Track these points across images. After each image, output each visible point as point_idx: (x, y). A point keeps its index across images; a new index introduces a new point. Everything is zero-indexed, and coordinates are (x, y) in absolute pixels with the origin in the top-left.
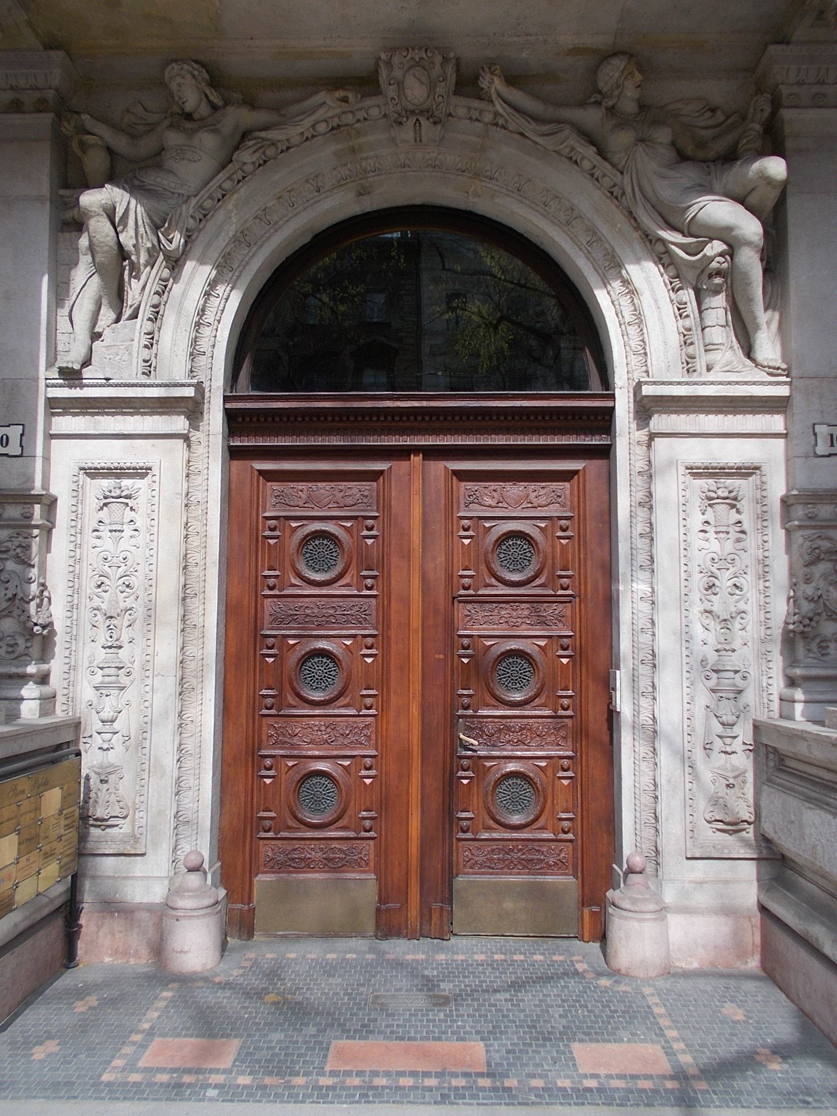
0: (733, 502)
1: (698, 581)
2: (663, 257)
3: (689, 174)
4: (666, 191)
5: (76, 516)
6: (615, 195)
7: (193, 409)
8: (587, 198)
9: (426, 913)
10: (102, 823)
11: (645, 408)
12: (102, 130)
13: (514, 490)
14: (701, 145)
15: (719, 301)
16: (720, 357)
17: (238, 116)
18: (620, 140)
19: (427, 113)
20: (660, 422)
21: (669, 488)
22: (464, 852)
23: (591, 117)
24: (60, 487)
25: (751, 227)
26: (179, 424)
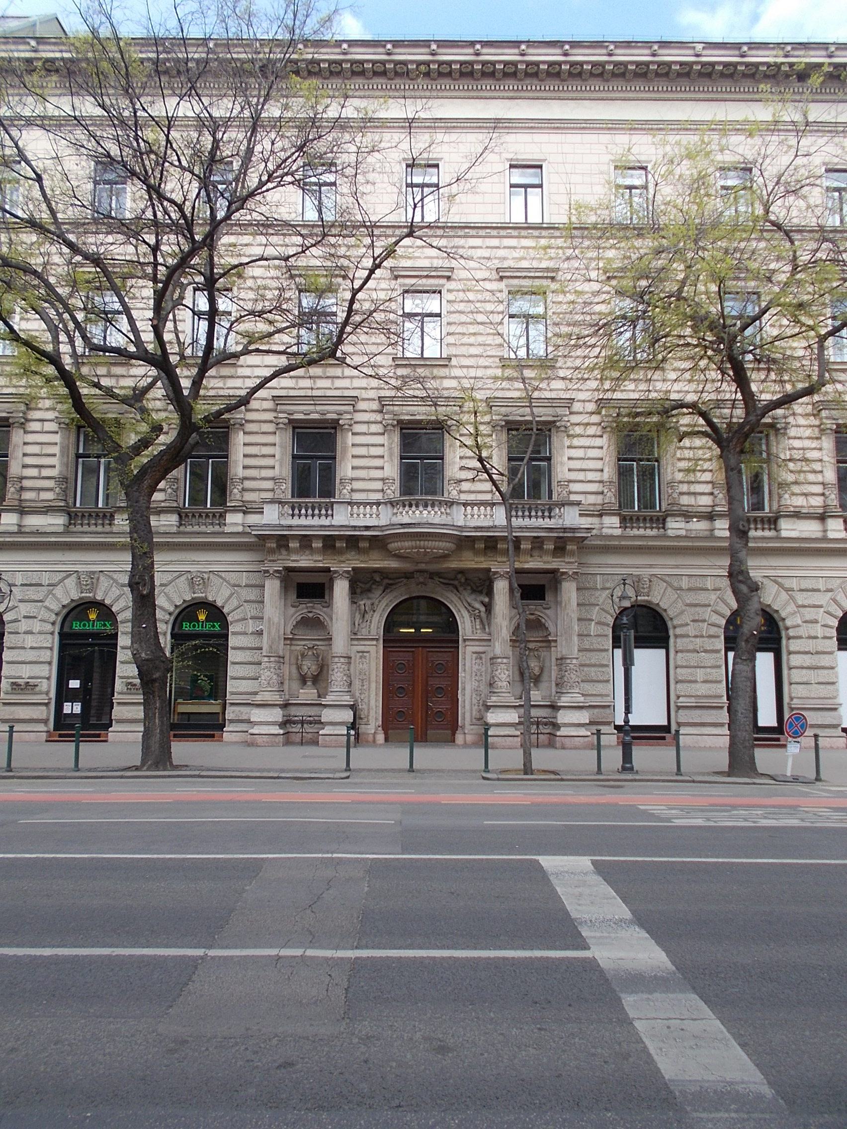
0: (481, 658)
1: (474, 674)
2: (468, 611)
3: (473, 596)
4: (469, 601)
5: (355, 661)
6: (460, 598)
7: (377, 640)
8: (455, 599)
9: (422, 738)
10: (361, 719)
11: (465, 640)
12: (360, 585)
13: (439, 654)
14: (477, 587)
15: (478, 621)
16: (479, 631)
17: (386, 581)
18: (461, 589)
19: (422, 583)
20: (467, 643)
21: (468, 657)
22: (429, 727)
23: (456, 583)
24: (352, 655)
25: (483, 609)
26: (374, 643)
